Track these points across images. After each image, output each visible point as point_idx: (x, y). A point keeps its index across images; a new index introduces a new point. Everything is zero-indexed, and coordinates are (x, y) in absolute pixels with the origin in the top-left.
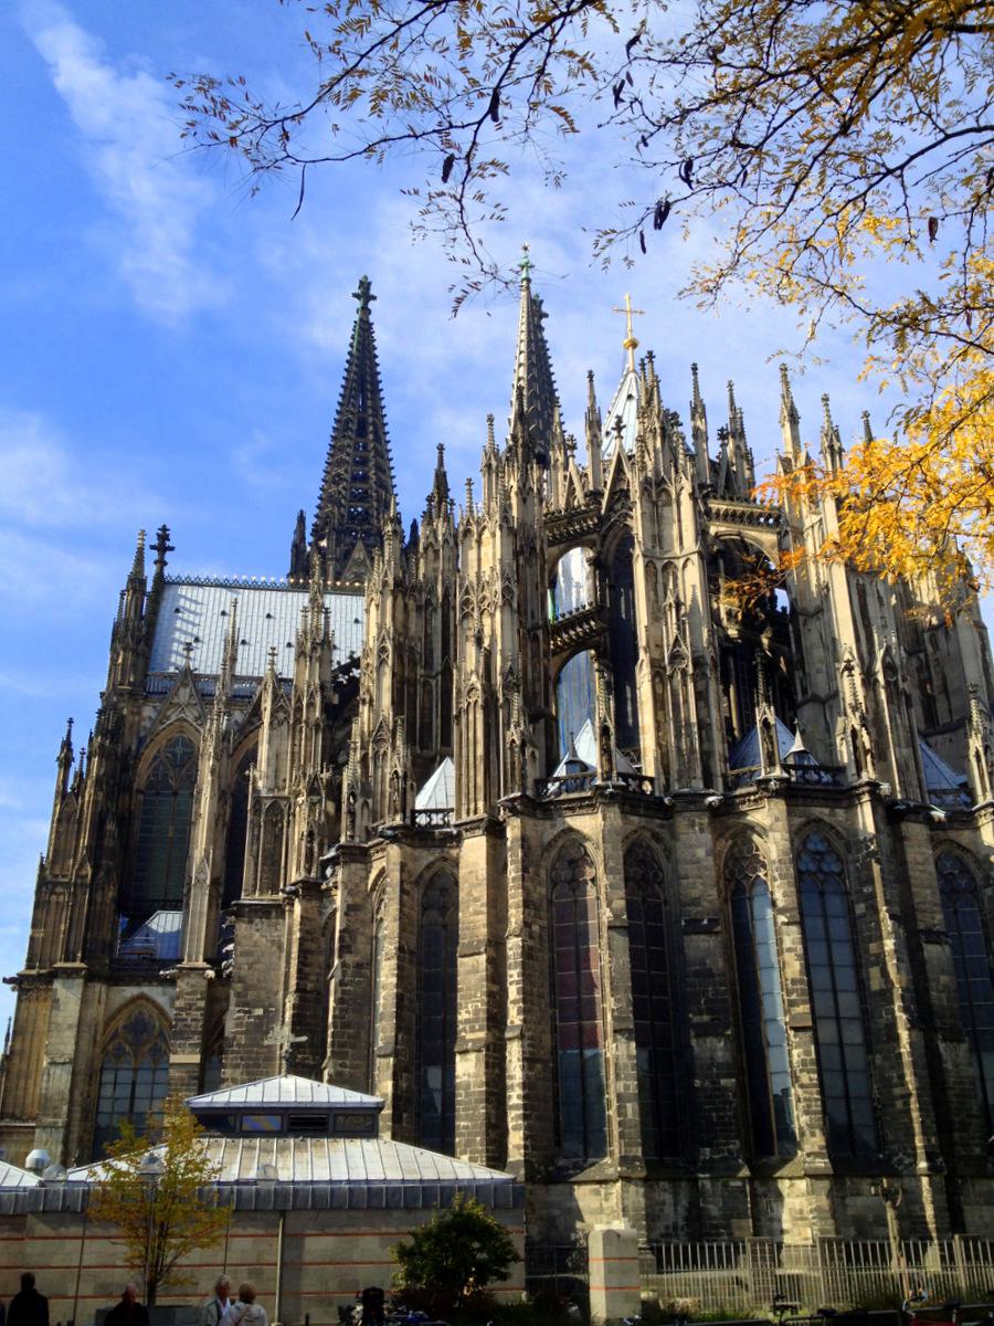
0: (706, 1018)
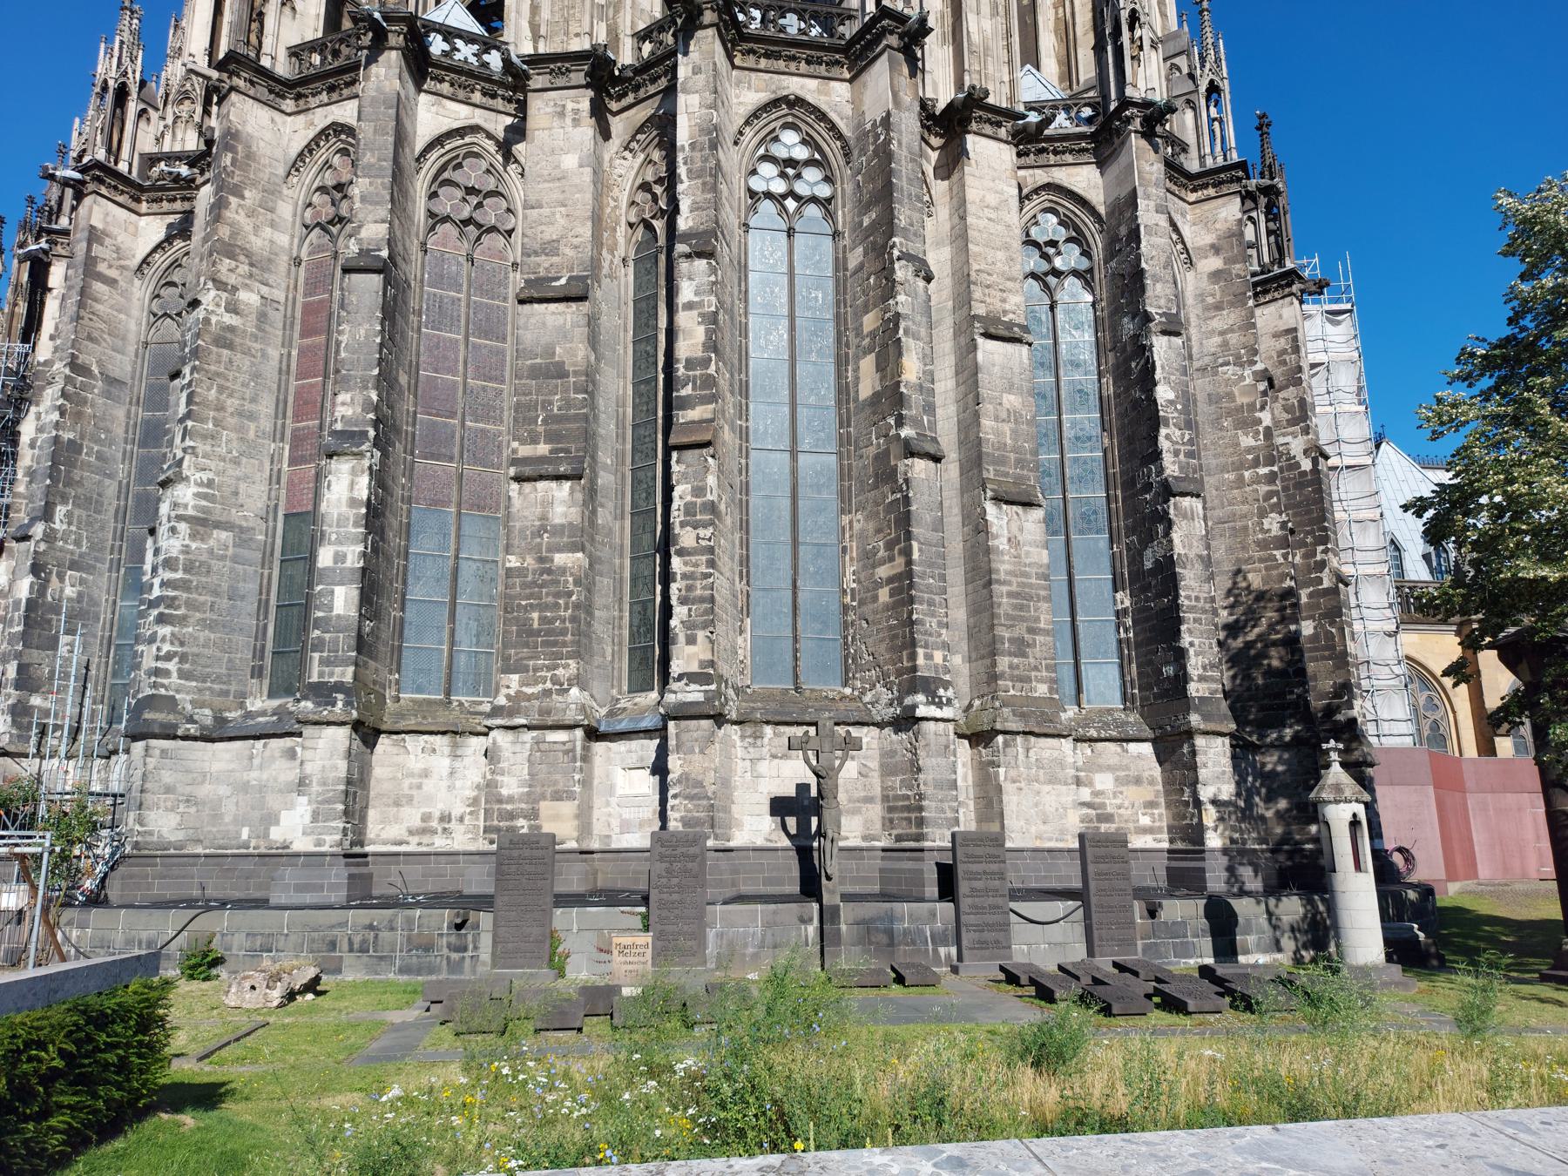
0: (543, 449)
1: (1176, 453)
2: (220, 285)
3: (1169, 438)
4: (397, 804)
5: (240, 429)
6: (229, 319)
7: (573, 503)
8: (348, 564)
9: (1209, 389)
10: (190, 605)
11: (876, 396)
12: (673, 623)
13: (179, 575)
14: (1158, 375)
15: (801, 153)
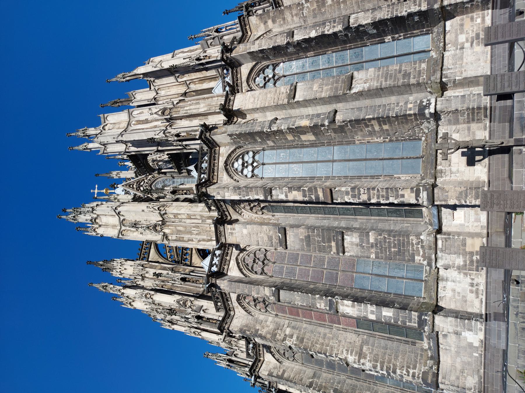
0: (333, 244)
1: (334, 27)
2: (284, 339)
3: (328, 30)
4: (466, 301)
5: (329, 339)
6: (295, 338)
7: (352, 235)
8: (375, 310)
9: (311, 18)
10: (389, 362)
11: (315, 134)
12: (396, 202)
13: (379, 364)
14: (307, 37)
15: (240, 161)
